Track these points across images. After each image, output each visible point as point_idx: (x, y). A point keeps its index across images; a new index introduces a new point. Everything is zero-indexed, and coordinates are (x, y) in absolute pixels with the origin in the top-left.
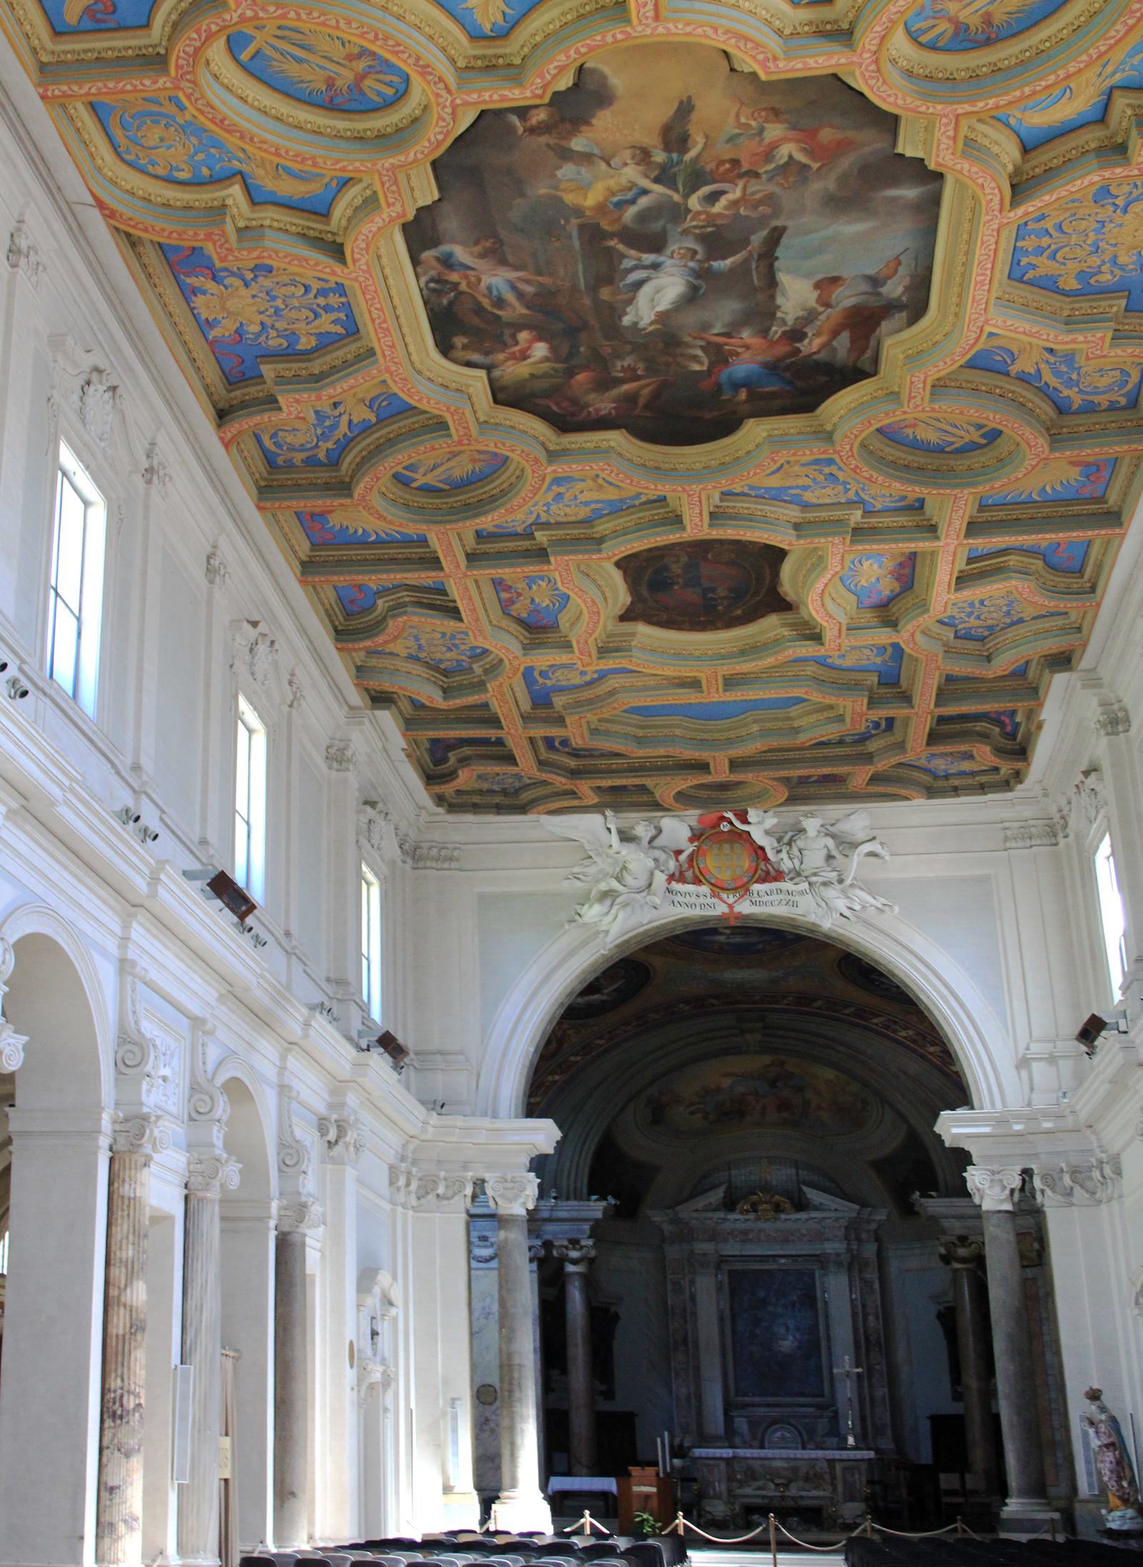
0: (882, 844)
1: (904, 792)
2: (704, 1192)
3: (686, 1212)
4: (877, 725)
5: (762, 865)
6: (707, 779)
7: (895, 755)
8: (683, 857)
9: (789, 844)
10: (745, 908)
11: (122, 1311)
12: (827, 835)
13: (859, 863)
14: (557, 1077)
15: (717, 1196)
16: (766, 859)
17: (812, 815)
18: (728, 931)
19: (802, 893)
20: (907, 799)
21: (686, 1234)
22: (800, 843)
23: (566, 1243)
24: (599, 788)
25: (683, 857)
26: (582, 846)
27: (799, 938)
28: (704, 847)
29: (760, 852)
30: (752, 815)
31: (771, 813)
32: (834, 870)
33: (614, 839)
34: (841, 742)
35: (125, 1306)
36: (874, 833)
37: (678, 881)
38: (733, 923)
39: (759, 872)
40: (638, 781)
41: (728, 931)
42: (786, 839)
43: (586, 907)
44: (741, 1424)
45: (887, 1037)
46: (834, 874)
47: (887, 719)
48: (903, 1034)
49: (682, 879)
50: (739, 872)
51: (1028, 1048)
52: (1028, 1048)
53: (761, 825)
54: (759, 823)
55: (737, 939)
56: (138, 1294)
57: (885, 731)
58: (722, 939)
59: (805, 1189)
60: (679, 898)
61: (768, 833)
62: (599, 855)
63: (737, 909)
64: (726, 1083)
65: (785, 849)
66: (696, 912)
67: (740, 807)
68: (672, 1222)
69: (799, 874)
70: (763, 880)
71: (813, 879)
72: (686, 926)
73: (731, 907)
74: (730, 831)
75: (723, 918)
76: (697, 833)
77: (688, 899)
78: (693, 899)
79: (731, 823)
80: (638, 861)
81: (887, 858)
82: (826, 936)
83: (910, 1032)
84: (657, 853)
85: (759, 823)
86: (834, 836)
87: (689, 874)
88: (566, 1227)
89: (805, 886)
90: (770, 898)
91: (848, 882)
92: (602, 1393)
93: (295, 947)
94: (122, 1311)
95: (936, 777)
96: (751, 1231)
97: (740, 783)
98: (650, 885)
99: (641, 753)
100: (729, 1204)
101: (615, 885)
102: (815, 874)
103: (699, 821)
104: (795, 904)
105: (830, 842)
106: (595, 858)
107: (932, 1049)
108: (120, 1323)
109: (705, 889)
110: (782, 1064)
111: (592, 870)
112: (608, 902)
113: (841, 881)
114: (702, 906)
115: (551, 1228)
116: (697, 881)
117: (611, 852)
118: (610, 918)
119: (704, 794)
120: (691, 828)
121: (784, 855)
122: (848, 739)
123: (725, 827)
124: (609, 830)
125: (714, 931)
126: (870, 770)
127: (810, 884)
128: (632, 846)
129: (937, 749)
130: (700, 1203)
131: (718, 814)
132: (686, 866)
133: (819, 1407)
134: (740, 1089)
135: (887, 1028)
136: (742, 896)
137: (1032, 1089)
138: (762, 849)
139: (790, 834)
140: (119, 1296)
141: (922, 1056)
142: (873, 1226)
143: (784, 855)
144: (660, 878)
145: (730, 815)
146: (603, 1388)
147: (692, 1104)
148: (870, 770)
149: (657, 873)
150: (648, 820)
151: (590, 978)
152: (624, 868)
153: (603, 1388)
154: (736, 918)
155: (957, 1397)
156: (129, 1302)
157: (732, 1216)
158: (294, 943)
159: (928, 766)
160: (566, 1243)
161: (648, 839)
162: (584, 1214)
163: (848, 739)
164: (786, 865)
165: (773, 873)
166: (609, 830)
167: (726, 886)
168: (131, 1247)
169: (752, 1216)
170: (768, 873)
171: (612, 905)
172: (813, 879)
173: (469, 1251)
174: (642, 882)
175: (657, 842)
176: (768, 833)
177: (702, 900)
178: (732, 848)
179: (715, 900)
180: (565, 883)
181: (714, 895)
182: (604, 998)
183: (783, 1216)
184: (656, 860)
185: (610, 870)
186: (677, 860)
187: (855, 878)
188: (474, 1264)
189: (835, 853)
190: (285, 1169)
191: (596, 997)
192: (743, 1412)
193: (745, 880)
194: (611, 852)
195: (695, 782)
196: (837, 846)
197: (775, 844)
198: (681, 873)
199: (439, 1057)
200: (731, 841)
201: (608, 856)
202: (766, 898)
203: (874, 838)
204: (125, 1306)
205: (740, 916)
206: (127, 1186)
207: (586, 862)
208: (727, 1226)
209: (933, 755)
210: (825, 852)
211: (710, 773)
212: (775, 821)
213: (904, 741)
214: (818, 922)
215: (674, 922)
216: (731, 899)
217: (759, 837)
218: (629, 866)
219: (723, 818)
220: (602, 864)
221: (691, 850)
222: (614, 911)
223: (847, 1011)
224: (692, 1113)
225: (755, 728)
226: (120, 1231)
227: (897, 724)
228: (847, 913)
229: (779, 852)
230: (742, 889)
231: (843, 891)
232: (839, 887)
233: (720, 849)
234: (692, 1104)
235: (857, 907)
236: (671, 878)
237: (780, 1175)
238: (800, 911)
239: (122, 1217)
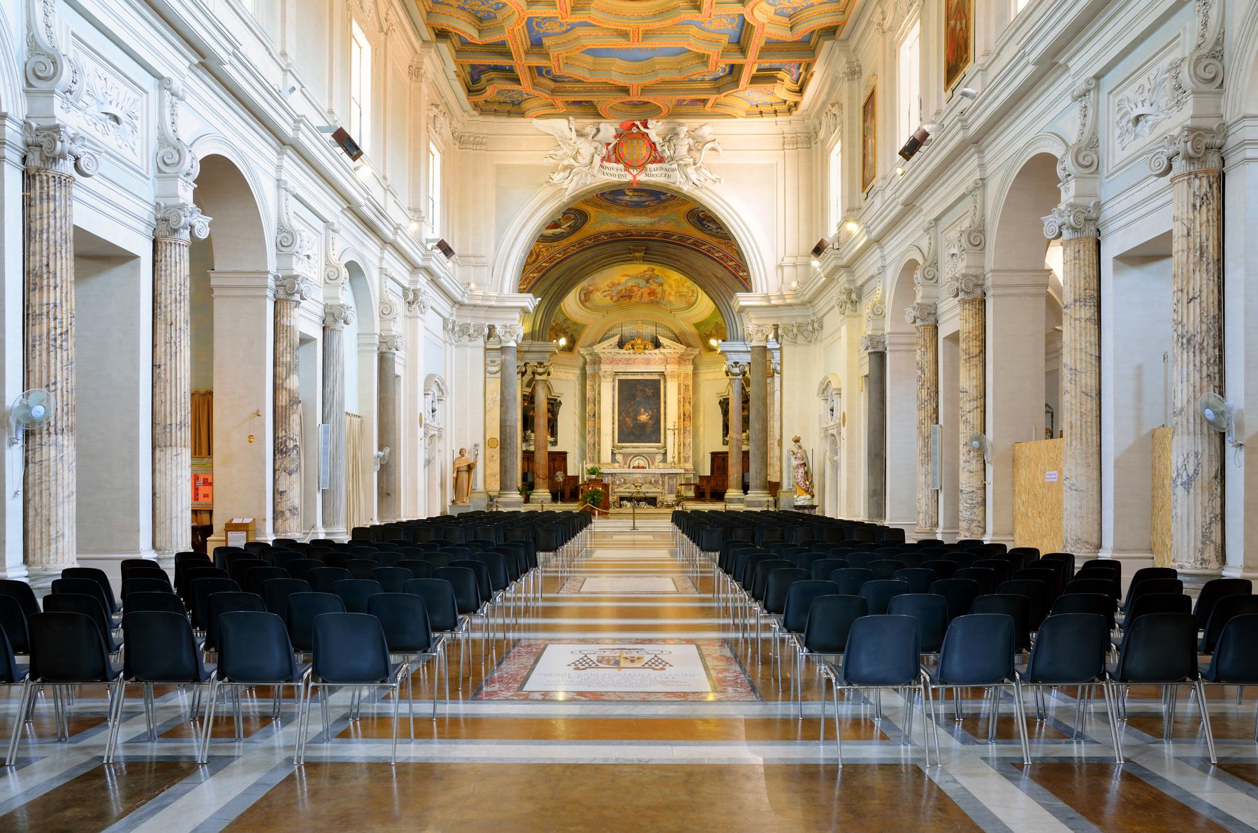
2: (609, 338)
3: (598, 348)
8: (610, 147)
9: (669, 141)
10: (642, 178)
11: (284, 392)
14: (535, 275)
15: (616, 339)
16: (656, 150)
21: (597, 361)
23: (536, 364)
25: (610, 147)
30: (651, 123)
32: (692, 157)
35: (286, 390)
37: (607, 161)
42: (667, 138)
44: (619, 457)
45: (710, 257)
48: (717, 255)
49: (609, 160)
51: (783, 260)
52: (783, 260)
53: (655, 129)
56: (294, 382)
59: (659, 337)
60: (607, 171)
62: (564, 144)
63: (638, 178)
64: (623, 280)
68: (591, 354)
69: (672, 159)
71: (681, 162)
77: (612, 172)
78: (614, 172)
80: (586, 148)
83: (721, 254)
88: (536, 356)
89: (675, 166)
90: (656, 172)
92: (551, 442)
93: (389, 186)
94: (284, 392)
96: (630, 359)
98: (592, 162)
100: (621, 345)
101: (572, 162)
107: (730, 263)
108: (283, 399)
109: (621, 166)
110: (653, 270)
111: (560, 153)
112: (568, 171)
114: (619, 176)
115: (529, 356)
116: (618, 161)
117: (571, 142)
121: (666, 148)
128: (583, 139)
130: (606, 344)
133: (658, 448)
134: (630, 284)
135: (709, 251)
136: (641, 171)
137: (782, 283)
138: (654, 143)
140: (282, 383)
141: (725, 267)
142: (692, 357)
143: (666, 148)
144: (597, 159)
146: (552, 439)
147: (605, 291)
150: (593, 124)
152: (578, 152)
153: (552, 439)
155: (725, 443)
156: (288, 387)
157: (622, 351)
158: (389, 183)
160: (536, 364)
162: (546, 349)
164: (667, 153)
165: (659, 158)
168: (288, 355)
169: (631, 351)
170: (656, 158)
172: (681, 162)
173: (485, 369)
174: (587, 160)
177: (619, 172)
178: (638, 143)
179: (626, 173)
180: (545, 160)
181: (626, 170)
182: (563, 231)
183: (647, 352)
184: (596, 148)
185: (570, 153)
188: (488, 375)
190: (383, 316)
192: (621, 451)
194: (571, 142)
199: (472, 259)
200: (639, 139)
204: (286, 390)
206: (285, 319)
207: (557, 148)
208: (619, 357)
216: (635, 172)
217: (654, 137)
220: (566, 150)
223: (689, 242)
224: (605, 296)
226: (282, 345)
230: (641, 167)
232: (693, 167)
233: (632, 142)
234: (605, 291)
236: (603, 159)
237: (649, 330)
238: (671, 180)
239: (283, 338)
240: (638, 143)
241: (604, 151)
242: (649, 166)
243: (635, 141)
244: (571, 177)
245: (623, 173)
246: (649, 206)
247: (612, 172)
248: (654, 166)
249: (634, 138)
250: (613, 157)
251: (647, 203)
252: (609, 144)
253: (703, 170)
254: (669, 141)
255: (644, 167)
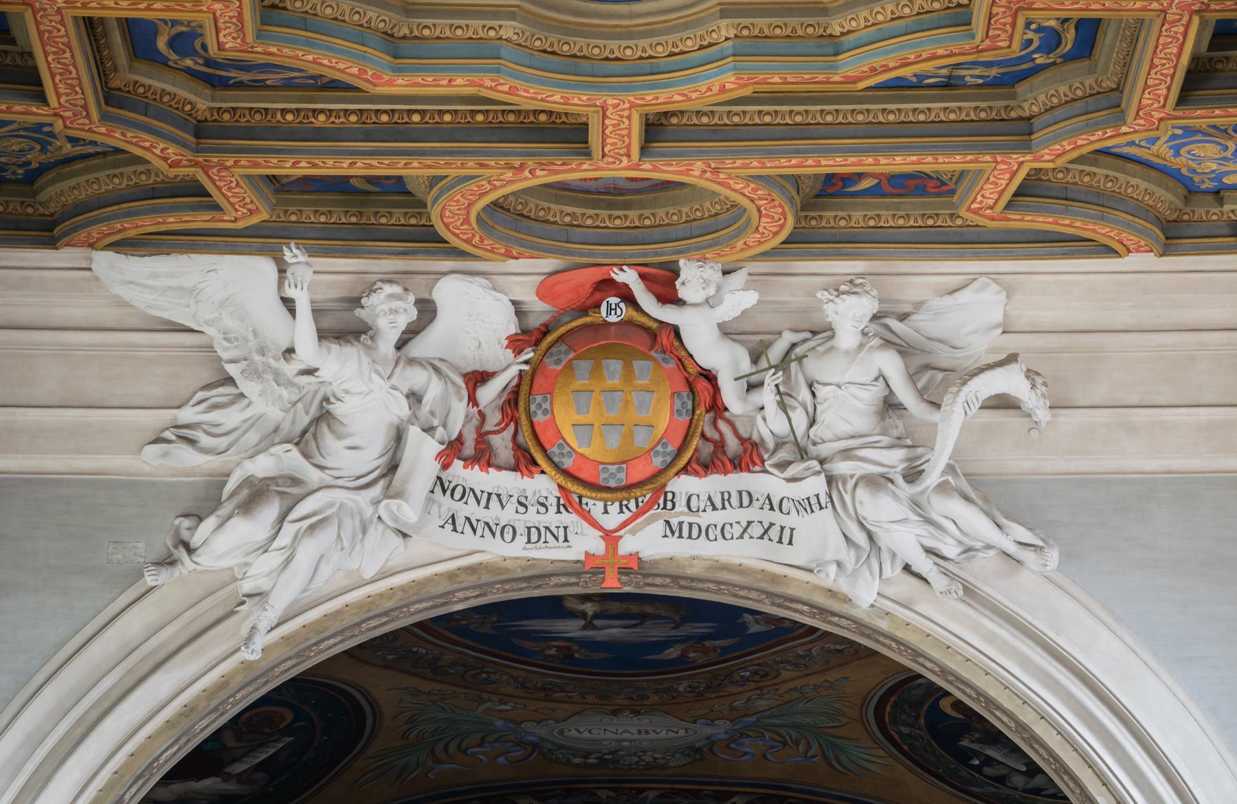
0: (1030, 374)
1: (1101, 231)
4: (1052, 39)
5: (705, 422)
6: (577, 171)
7: (1090, 128)
8: (489, 393)
9: (783, 364)
12: (888, 343)
13: (965, 428)
16: (717, 408)
17: (853, 286)
18: (589, 608)
19: (807, 506)
20: (1108, 251)
22: (815, 367)
24: (273, 179)
25: (489, 393)
26: (210, 348)
27: (784, 631)
28: (551, 365)
29: (703, 385)
31: (739, 278)
33: (304, 330)
34: (950, 85)
36: (1014, 343)
37: (469, 461)
38: (612, 583)
39: (696, 442)
40: (382, 167)
41: (589, 608)
42: (775, 353)
43: (210, 523)
46: (895, 458)
47: (1080, 24)
49: (483, 457)
50: (642, 439)
54: (709, 303)
55: (614, 632)
57: (1069, 58)
58: (571, 628)
60: (471, 509)
61: (727, 331)
63: (628, 545)
65: (770, 379)
66: (514, 551)
67: (658, 254)
69: (803, 454)
70: (705, 466)
72: (483, 588)
73: (611, 538)
74: (627, 323)
75: (590, 567)
76: (534, 322)
77: (494, 513)
78: (508, 515)
79: (628, 297)
81: (1043, 415)
82: (861, 626)
84: (417, 377)
85: (709, 303)
86: (904, 350)
87: (502, 444)
89: (815, 485)
90: (719, 517)
91: (933, 477)
95: (1191, 192)
97: (667, 185)
99: (401, 85)
102: (847, 454)
103: (543, 292)
104: (787, 537)
105: (891, 364)
106: (245, 386)
109: (543, 485)
111: (230, 417)
112: (269, 512)
113: (913, 475)
114: (535, 534)
116: (524, 462)
118: (273, 559)
119: (562, 212)
120: (519, 310)
121: (767, 397)
122: (970, 75)
123: (612, 311)
124: (289, 304)
125: (554, 606)
126: (1021, 164)
127: (830, 480)
129: (1200, 117)
131: (595, 275)
132: (494, 419)
138: (709, 377)
139: (788, 338)
143: (767, 397)
145: (628, 277)
148: (1021, 164)
149: (414, 432)
151: (205, 728)
152: (324, 416)
154: (624, 571)
159: (1182, 162)
161: (394, 336)
163: (970, 75)
165: (732, 444)
166: (289, 304)
167: (602, 479)
170: (720, 445)
171: (282, 519)
172: (842, 467)
174: (370, 458)
175: (422, 347)
176: (727, 331)
177: (532, 517)
178: (629, 374)
179: (570, 518)
181: (567, 503)
182: (231, 787)
184: (415, 397)
186: (472, 400)
187: (950, 469)
189: (905, 394)
191: (210, 784)
193: (658, 462)
195: (543, 177)
196: (913, 377)
197: (746, 366)
198: (482, 438)
200: (628, 355)
201: (278, 378)
202: (706, 519)
203: (1012, 359)
205: (636, 567)
209: (1189, 131)
210: (878, 391)
211: (587, 154)
212: (750, 298)
213: (1119, 89)
214: (843, 586)
215: (451, 576)
216: (612, 519)
218: (337, 409)
219: (607, 285)
221: (513, 371)
222: (289, 530)
225: (725, 29)
227: (1108, 41)
228: (924, 565)
229: (752, 387)
231: (916, 505)
232: (905, 490)
233: (596, 372)
235: (951, 550)
236: (452, 450)
238: (796, 554)
240: (629, 374)
241: (460, 410)
242: (683, 485)
243: (614, 366)
244: (284, 539)
245: (552, 518)
246: (681, 664)
247: (494, 513)
248: (713, 484)
249: (610, 351)
250: (502, 444)
251: (673, 653)
252: (477, 378)
253: (956, 507)
254: (783, 364)
255: (661, 491)
